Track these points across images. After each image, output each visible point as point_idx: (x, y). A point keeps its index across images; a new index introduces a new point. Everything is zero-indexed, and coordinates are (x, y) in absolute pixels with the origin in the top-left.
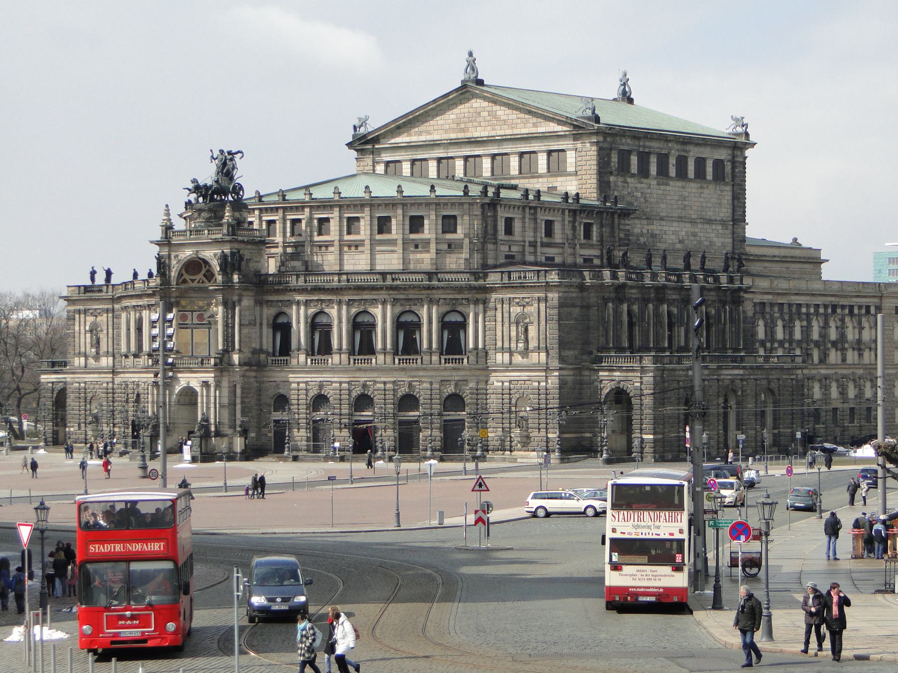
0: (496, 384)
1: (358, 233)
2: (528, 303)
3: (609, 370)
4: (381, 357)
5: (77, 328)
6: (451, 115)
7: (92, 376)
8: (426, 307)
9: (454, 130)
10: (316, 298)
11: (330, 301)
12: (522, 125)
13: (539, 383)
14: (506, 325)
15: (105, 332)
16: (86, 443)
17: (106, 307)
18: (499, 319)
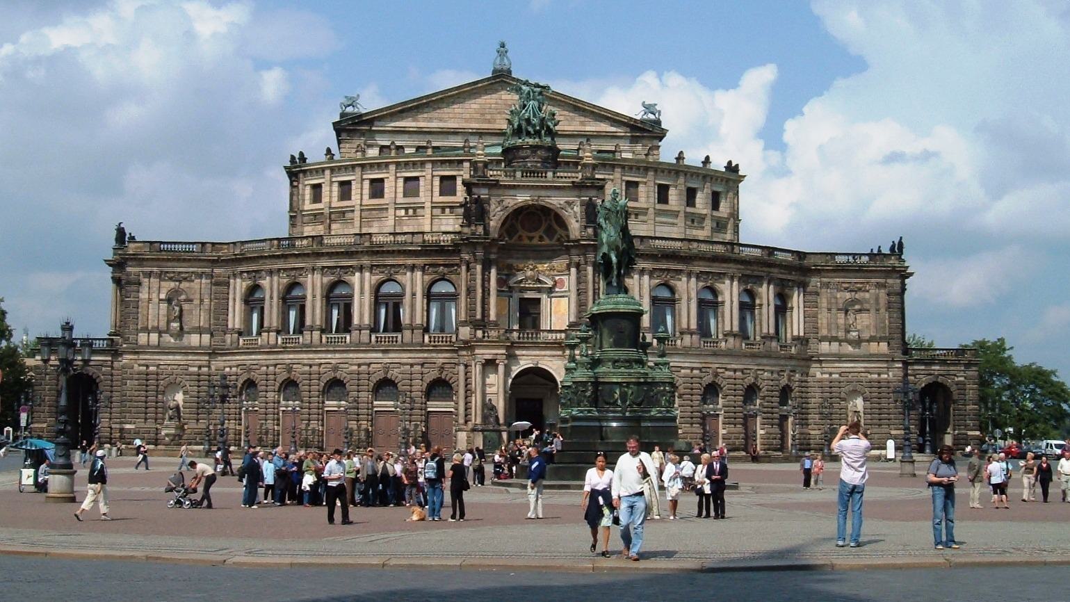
0: (819, 375)
1: (636, 200)
2: (860, 289)
3: (926, 364)
4: (731, 340)
5: (144, 295)
6: (474, 105)
7: (171, 357)
8: (765, 285)
9: (477, 121)
10: (664, 267)
11: (679, 272)
12: (567, 123)
13: (879, 374)
14: (834, 311)
15: (197, 302)
16: (156, 445)
17: (200, 270)
18: (825, 305)
